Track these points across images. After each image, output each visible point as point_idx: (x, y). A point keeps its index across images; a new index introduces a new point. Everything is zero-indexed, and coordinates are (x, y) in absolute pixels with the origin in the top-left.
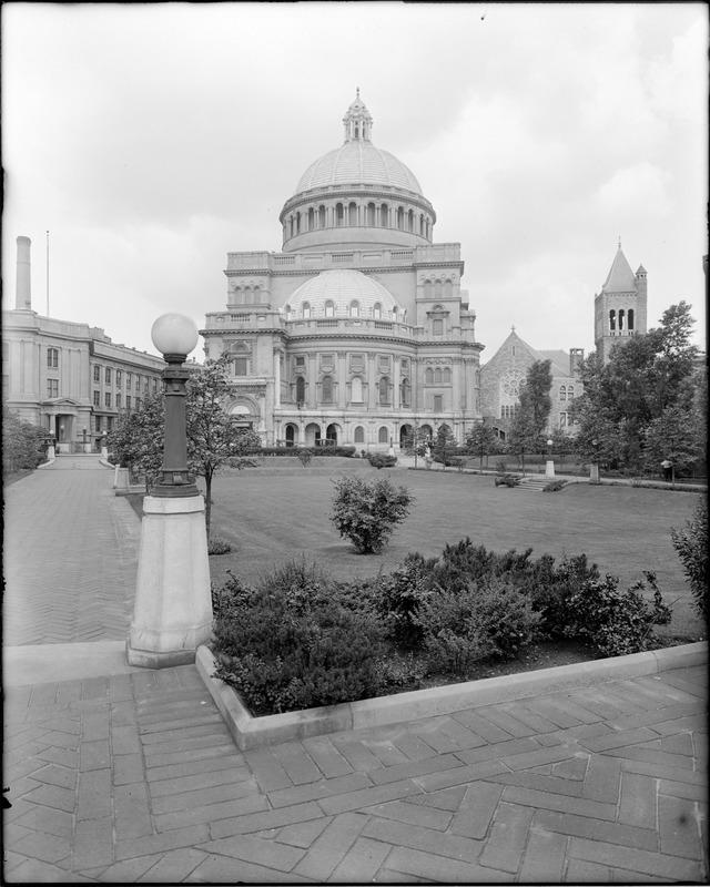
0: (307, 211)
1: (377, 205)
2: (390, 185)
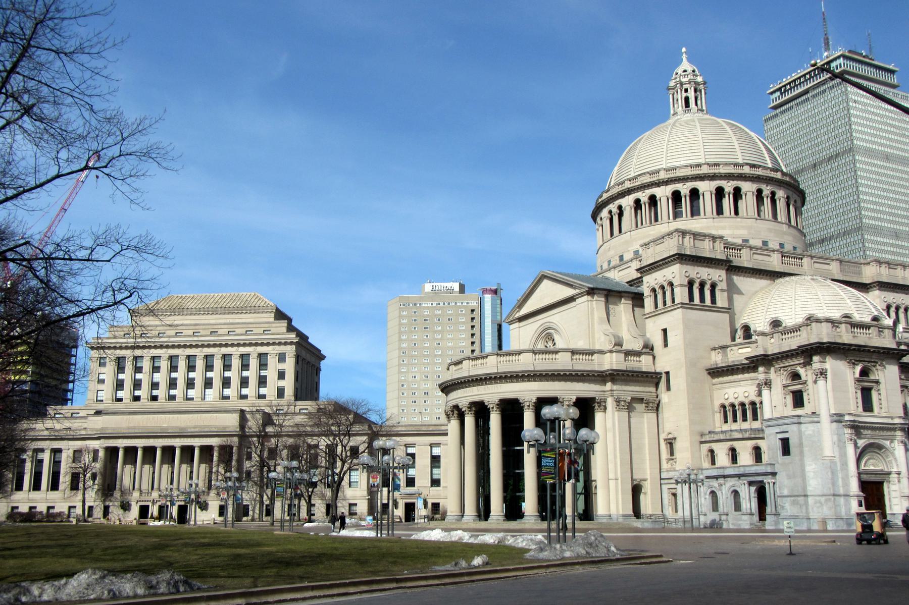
0: (632, 203)
2: (740, 161)
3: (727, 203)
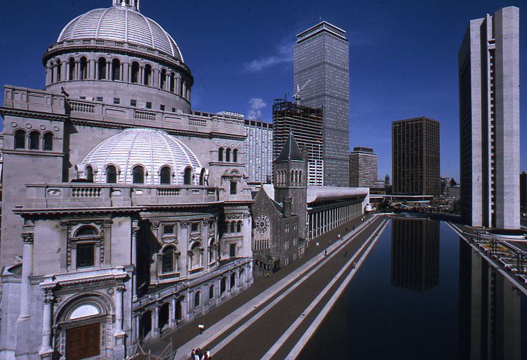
1: (141, 65)
3: (141, 74)
